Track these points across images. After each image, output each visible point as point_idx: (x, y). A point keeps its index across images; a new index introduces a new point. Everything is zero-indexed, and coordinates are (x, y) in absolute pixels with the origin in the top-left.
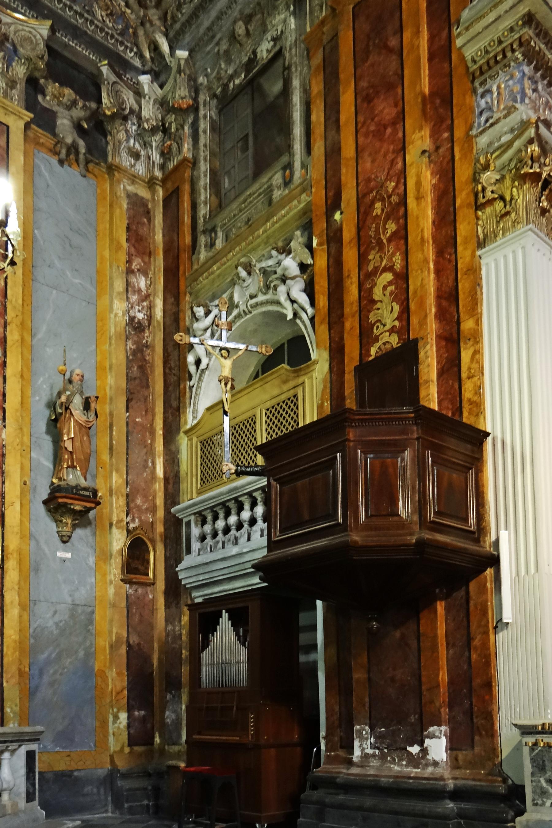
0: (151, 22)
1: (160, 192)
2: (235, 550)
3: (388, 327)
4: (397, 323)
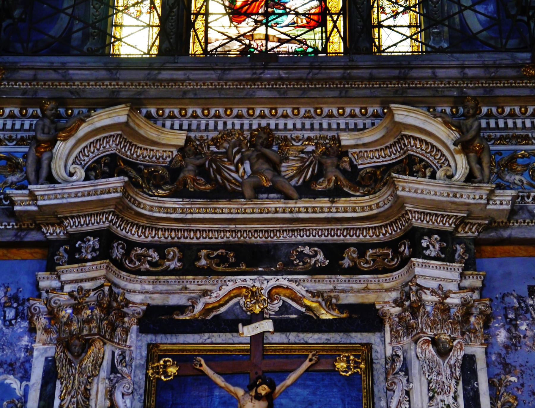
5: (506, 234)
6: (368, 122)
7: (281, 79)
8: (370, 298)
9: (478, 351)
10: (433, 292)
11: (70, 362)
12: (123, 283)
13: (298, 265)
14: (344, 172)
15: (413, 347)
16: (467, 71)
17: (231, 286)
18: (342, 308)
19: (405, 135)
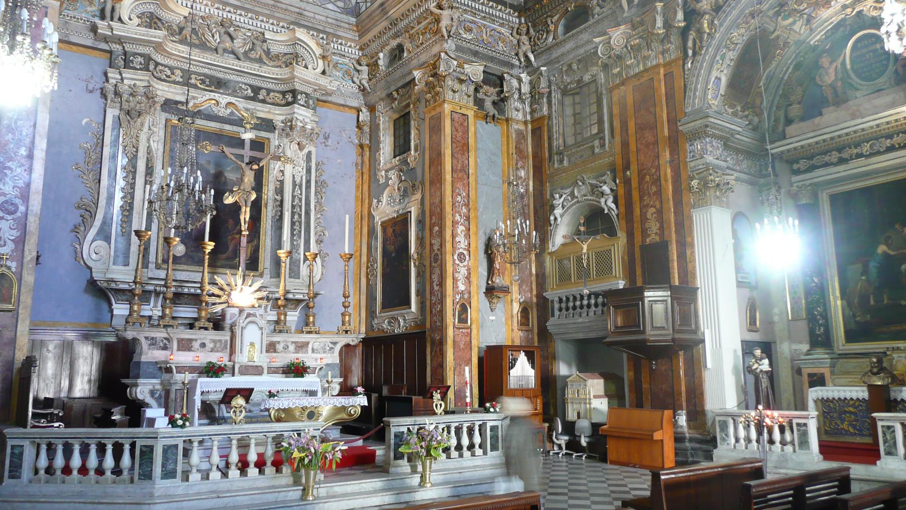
1: (530, 126)
2: (580, 320)
5: (330, 99)
6: (279, 29)
8: (270, 117)
9: (313, 149)
11: (129, 122)
12: (154, 85)
14: (264, 51)
17: (208, 97)
18: (258, 118)
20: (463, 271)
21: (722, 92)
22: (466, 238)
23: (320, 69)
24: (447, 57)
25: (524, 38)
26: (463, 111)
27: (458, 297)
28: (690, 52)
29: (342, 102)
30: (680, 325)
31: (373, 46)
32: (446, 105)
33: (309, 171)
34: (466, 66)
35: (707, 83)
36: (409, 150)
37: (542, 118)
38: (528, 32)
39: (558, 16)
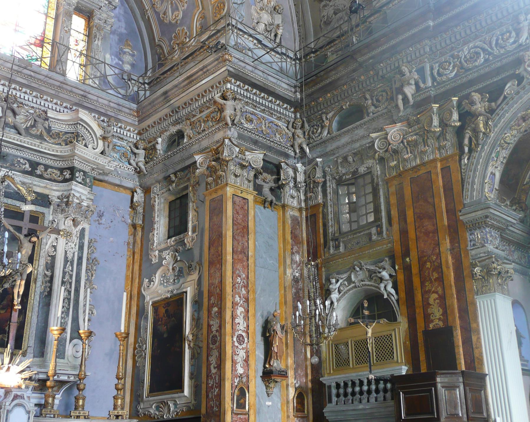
0: (298, 136)
1: (304, 213)
2: (361, 407)
3: (438, 317)
4: (441, 317)
5: (106, 178)
6: (62, 109)
7: (31, 76)
8: (46, 192)
9: (87, 226)
10: (78, 199)
13: (16, 166)
14: (45, 128)
15: (63, 219)
16: (111, 103)
19: (79, 123)
20: (242, 354)
21: (496, 186)
22: (245, 320)
23: (100, 148)
24: (230, 143)
25: (299, 132)
26: (244, 195)
27: (236, 381)
28: (466, 149)
29: (118, 182)
30: (473, 413)
31: (152, 131)
32: (228, 189)
33: (81, 248)
34: (247, 153)
35: (484, 178)
36: (186, 230)
37: (317, 205)
38: (302, 127)
39: (333, 113)
